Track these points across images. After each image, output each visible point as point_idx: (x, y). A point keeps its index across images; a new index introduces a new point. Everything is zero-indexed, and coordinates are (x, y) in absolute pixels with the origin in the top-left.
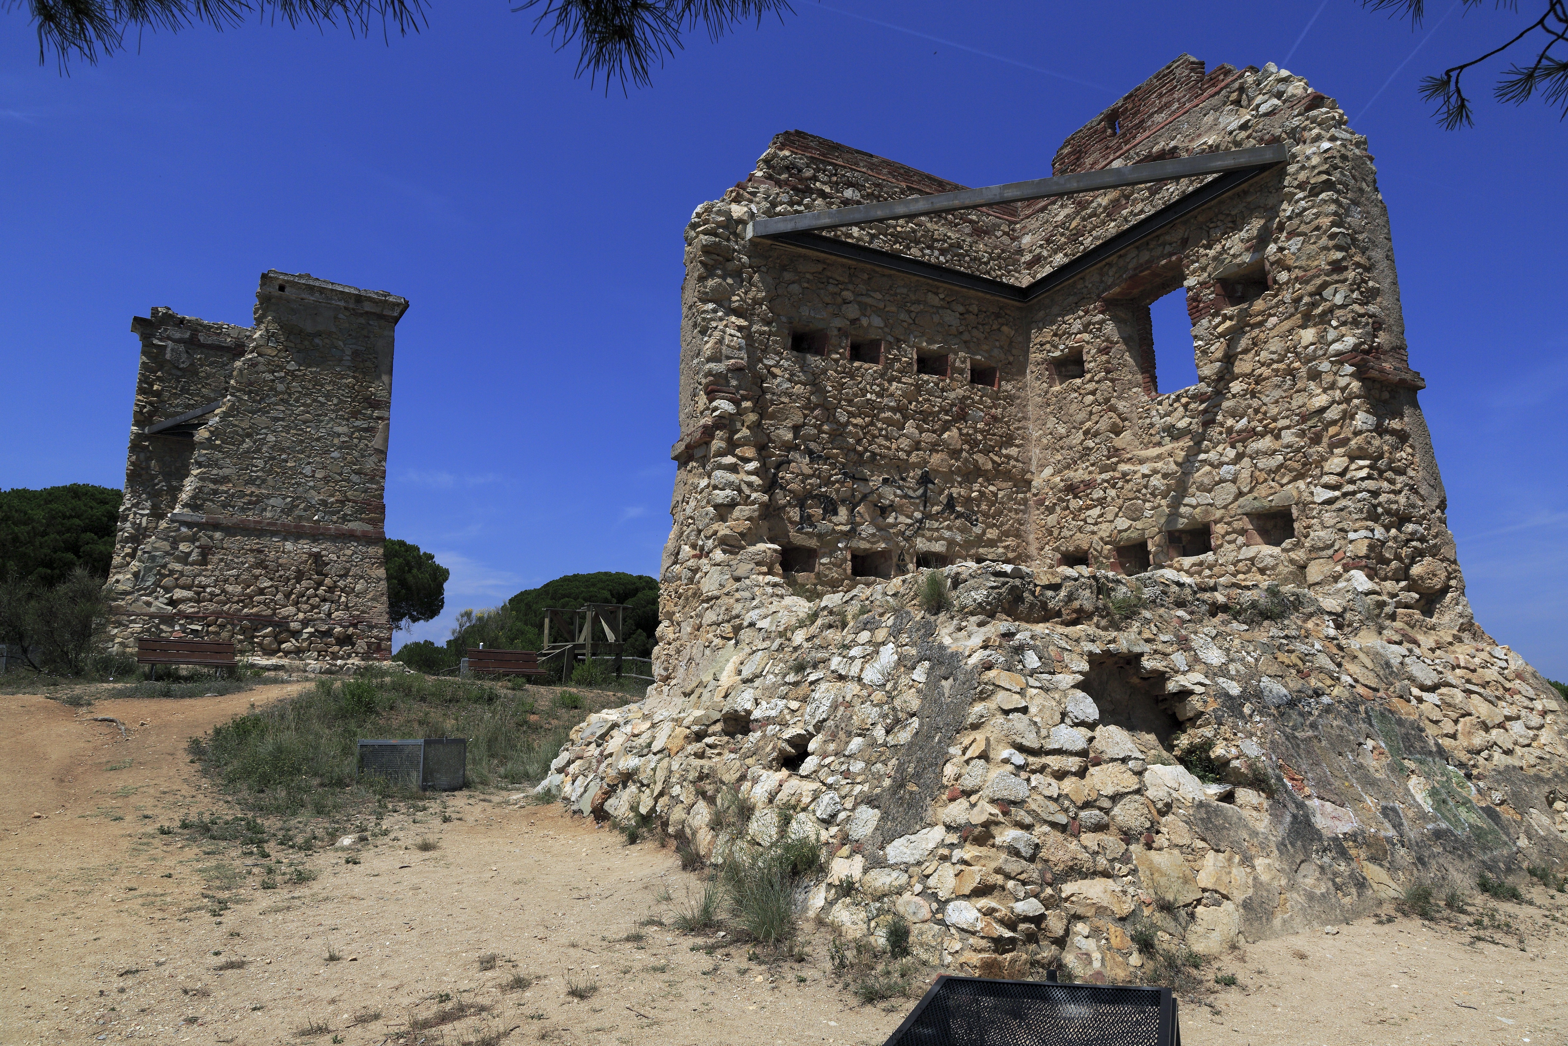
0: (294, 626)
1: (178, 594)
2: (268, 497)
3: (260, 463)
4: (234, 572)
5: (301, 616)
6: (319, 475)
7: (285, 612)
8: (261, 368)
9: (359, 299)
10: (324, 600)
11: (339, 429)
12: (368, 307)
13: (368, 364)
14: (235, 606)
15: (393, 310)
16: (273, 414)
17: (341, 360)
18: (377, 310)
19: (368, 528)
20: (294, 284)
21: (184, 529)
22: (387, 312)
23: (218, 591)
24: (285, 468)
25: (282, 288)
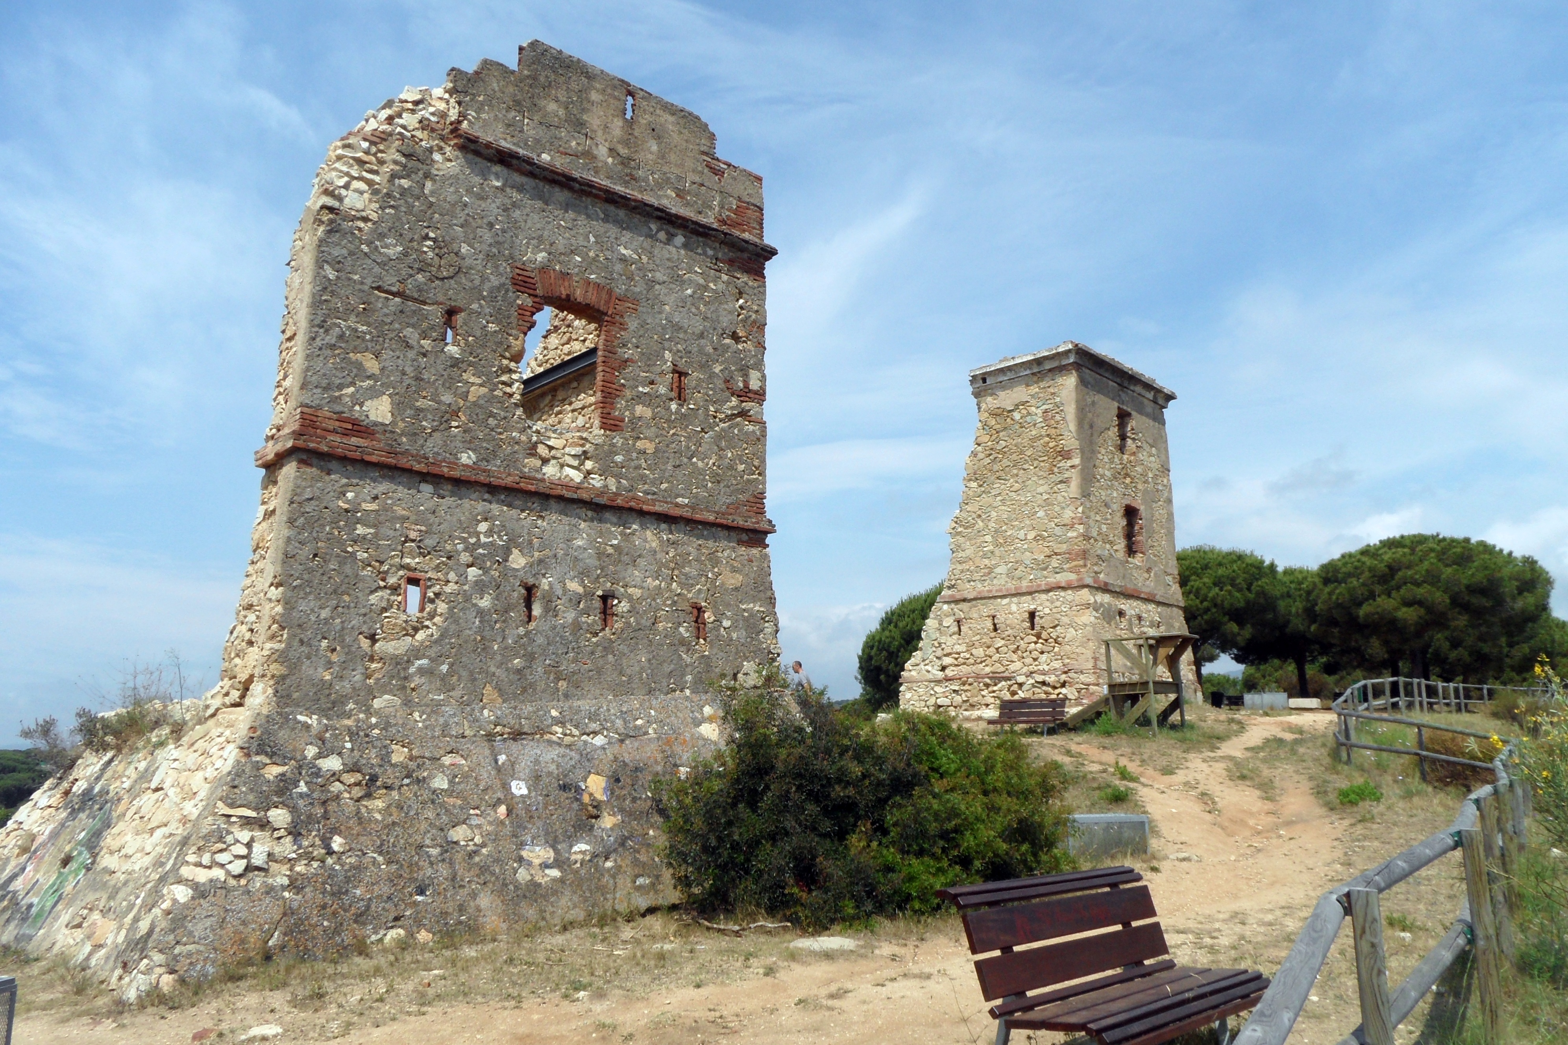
0: (1021, 679)
1: (947, 661)
2: (996, 566)
3: (988, 538)
4: (978, 637)
5: (1025, 670)
6: (1031, 535)
7: (1012, 667)
8: (981, 456)
9: (1039, 361)
10: (1042, 653)
11: (1040, 490)
12: (1048, 366)
13: (1058, 417)
14: (981, 666)
15: (1068, 358)
16: (994, 492)
17: (1035, 425)
18: (1055, 364)
19: (1073, 577)
20: (990, 373)
21: (945, 607)
22: (1064, 362)
23: (968, 656)
24: (1005, 538)
25: (984, 380)
